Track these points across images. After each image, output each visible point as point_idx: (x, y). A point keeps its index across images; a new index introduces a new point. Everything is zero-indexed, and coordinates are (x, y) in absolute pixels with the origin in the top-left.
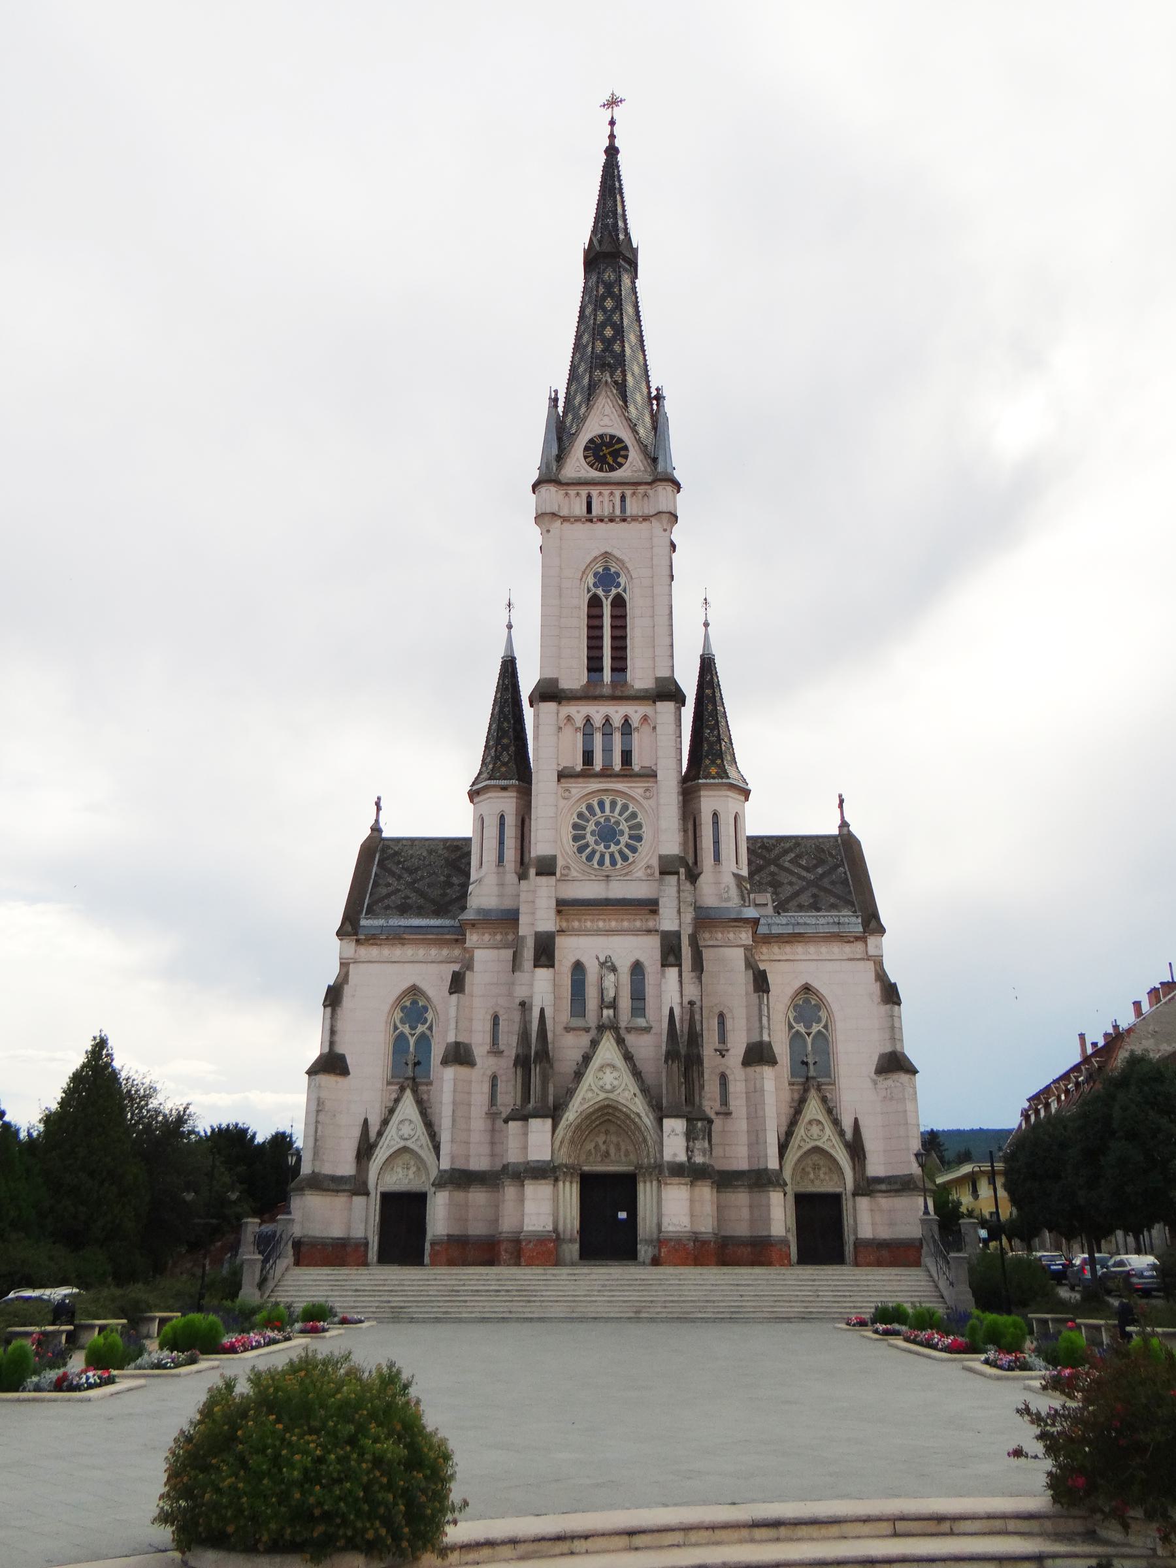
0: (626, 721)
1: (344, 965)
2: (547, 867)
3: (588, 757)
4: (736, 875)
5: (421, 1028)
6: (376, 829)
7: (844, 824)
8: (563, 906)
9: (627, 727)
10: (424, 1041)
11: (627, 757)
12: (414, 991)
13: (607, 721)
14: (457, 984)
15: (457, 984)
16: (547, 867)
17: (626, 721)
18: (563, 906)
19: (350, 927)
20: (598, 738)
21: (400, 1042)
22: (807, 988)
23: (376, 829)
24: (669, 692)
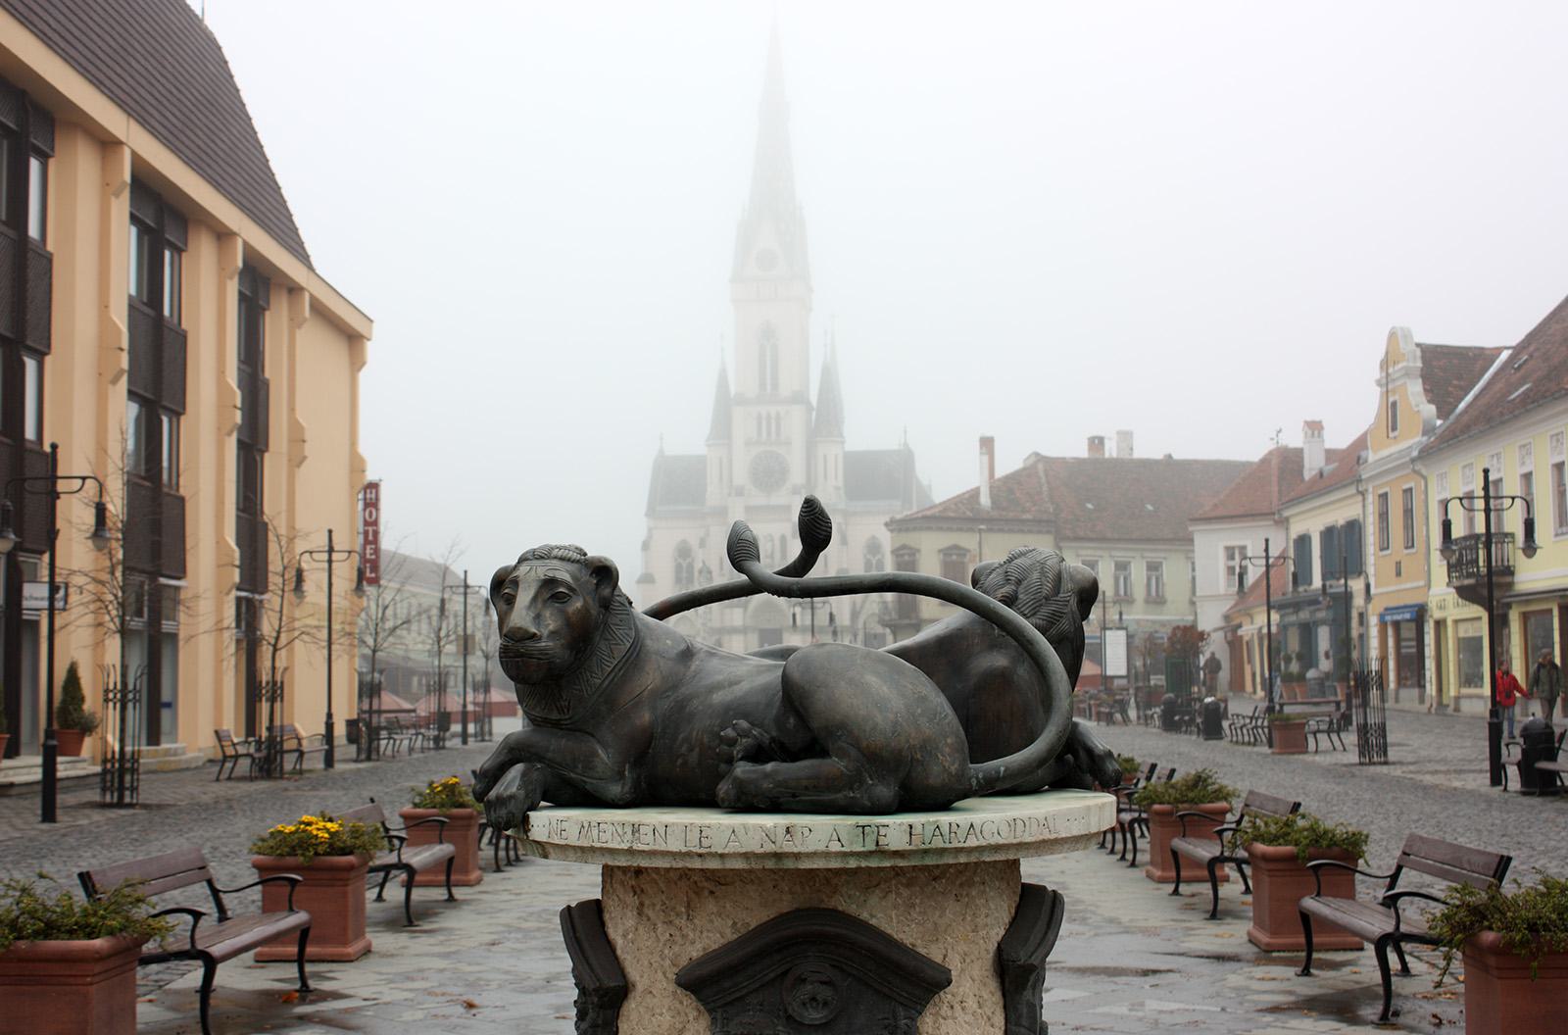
0: (778, 414)
1: (650, 530)
2: (740, 492)
3: (759, 433)
4: (837, 488)
5: (689, 560)
6: (661, 451)
7: (906, 444)
8: (748, 509)
9: (778, 418)
10: (691, 566)
11: (778, 434)
12: (684, 542)
13: (769, 417)
14: (702, 544)
15: (702, 544)
16: (740, 492)
17: (778, 414)
18: (748, 509)
19: (651, 512)
20: (764, 423)
21: (678, 568)
22: (874, 538)
23: (661, 451)
24: (800, 398)
